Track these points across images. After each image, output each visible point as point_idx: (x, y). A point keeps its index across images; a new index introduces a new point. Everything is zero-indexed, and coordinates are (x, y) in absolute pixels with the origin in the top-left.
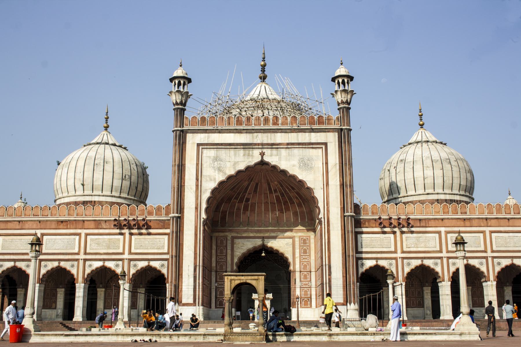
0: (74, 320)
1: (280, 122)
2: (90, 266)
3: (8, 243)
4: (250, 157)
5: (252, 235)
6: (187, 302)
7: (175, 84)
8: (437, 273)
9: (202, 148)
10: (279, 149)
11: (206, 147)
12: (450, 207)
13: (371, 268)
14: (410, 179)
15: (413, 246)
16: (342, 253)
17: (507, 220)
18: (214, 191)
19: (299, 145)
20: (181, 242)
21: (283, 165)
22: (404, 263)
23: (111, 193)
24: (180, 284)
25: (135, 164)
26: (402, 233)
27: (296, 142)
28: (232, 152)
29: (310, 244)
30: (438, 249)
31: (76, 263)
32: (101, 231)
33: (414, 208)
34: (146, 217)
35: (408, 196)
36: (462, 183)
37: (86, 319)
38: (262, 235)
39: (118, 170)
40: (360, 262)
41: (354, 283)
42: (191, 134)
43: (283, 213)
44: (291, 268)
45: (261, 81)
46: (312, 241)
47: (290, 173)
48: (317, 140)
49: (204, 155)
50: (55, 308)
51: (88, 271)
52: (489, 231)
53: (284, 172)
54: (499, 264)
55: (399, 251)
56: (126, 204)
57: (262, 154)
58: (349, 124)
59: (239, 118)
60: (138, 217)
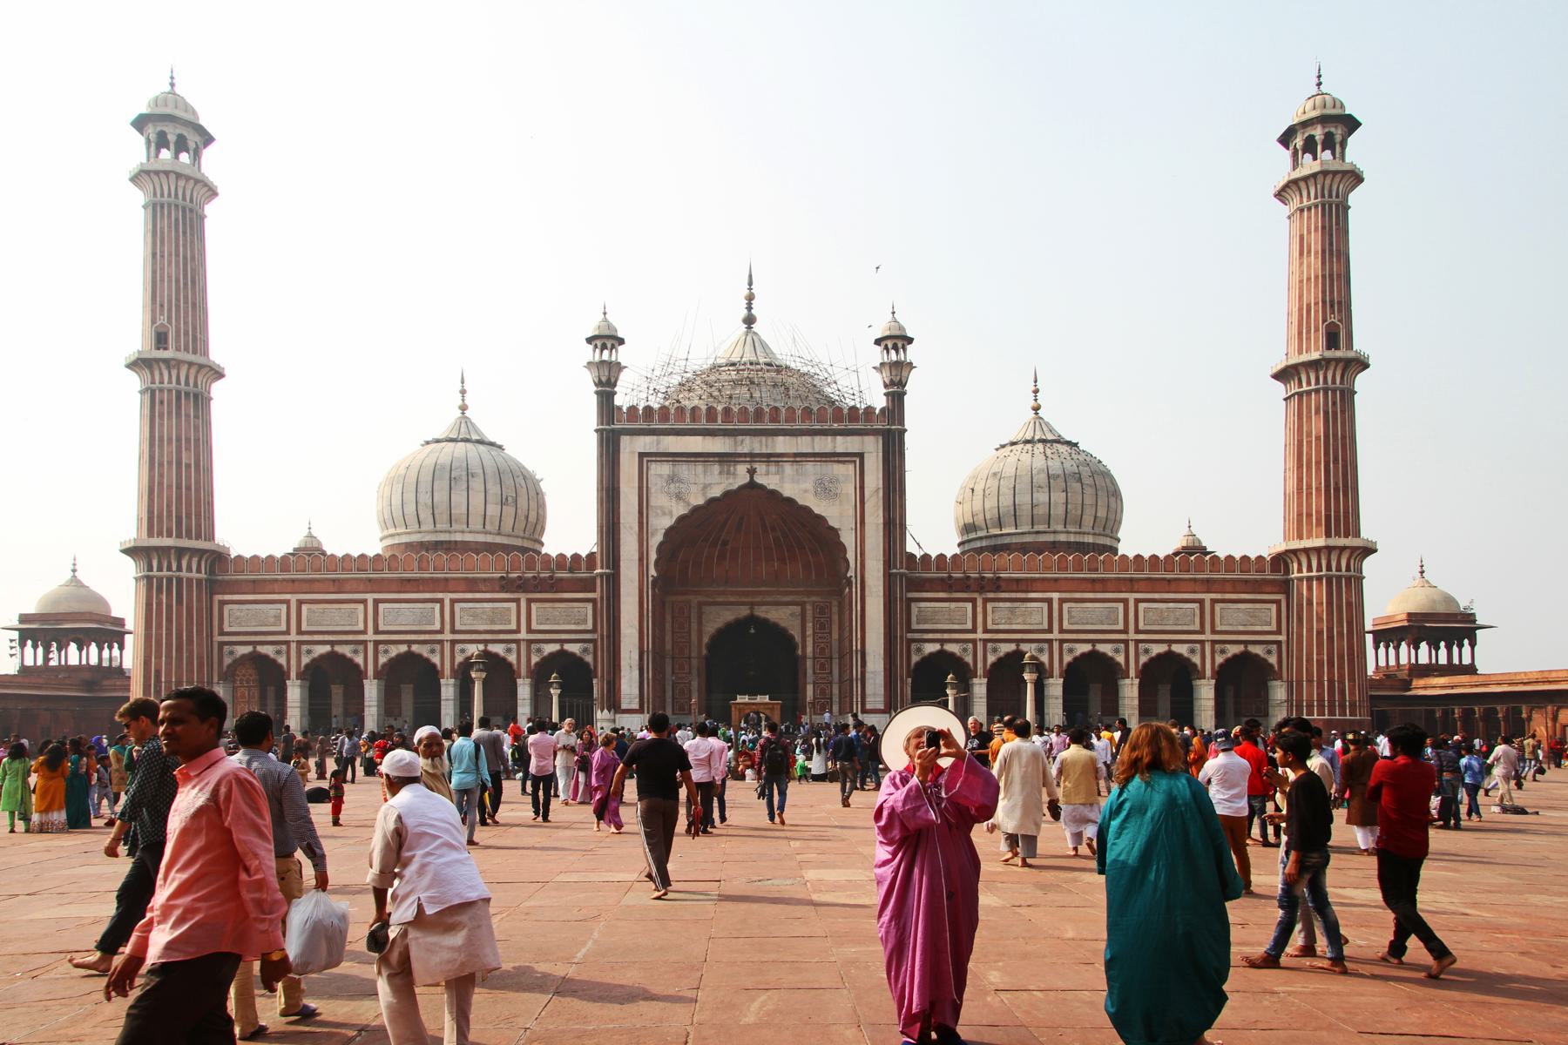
1: (783, 416)
3: (317, 615)
4: (732, 476)
13: (931, 654)
15: (1003, 621)
17: (1166, 582)
21: (788, 491)
24: (617, 681)
26: (986, 601)
27: (810, 451)
30: (1045, 626)
32: (478, 596)
34: (554, 573)
40: (914, 646)
47: (801, 502)
52: (1135, 599)
53: (790, 501)
54: (1147, 651)
55: (980, 629)
57: (752, 472)
60: (539, 573)
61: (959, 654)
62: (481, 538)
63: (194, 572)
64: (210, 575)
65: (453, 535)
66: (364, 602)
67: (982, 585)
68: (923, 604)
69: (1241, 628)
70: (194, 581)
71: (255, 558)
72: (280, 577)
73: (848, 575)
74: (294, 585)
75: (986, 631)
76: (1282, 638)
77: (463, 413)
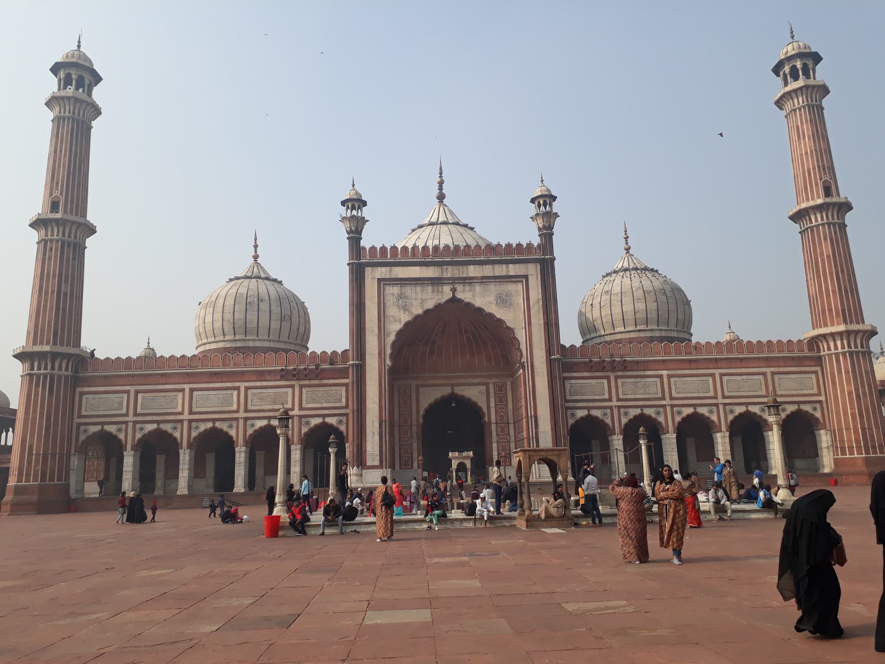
0: (234, 491)
2: (253, 425)
5: (440, 382)
6: (372, 465)
7: (348, 208)
8: (660, 423)
9: (384, 284)
10: (473, 284)
11: (388, 283)
12: (672, 347)
13: (582, 418)
14: (618, 313)
16: (550, 402)
18: (399, 333)
19: (495, 279)
20: (363, 394)
21: (478, 302)
22: (621, 412)
23: (269, 337)
24: (363, 445)
25: (294, 302)
26: (616, 378)
27: (492, 275)
28: (419, 288)
29: (506, 390)
30: (660, 395)
31: (234, 424)
32: (264, 384)
33: (630, 348)
35: (615, 333)
36: (679, 317)
37: (248, 489)
38: (451, 382)
39: (276, 309)
40: (569, 412)
41: (564, 437)
42: (370, 268)
43: (475, 356)
44: (486, 419)
45: (439, 202)
46: (509, 388)
48: (516, 273)
49: (387, 292)
50: (204, 477)
51: (250, 431)
52: (719, 373)
53: (480, 310)
54: (732, 411)
55: (614, 399)
56: (294, 351)
57: (454, 290)
58: (552, 253)
59: (426, 248)
61: (601, 417)
62: (266, 344)
63: (64, 371)
64: (75, 372)
65: (247, 342)
66: (182, 390)
67: (613, 367)
68: (573, 381)
69: (794, 392)
70: (63, 377)
71: (108, 359)
72: (124, 373)
73: (522, 361)
74: (133, 379)
75: (619, 400)
76: (822, 398)
77: (255, 260)
